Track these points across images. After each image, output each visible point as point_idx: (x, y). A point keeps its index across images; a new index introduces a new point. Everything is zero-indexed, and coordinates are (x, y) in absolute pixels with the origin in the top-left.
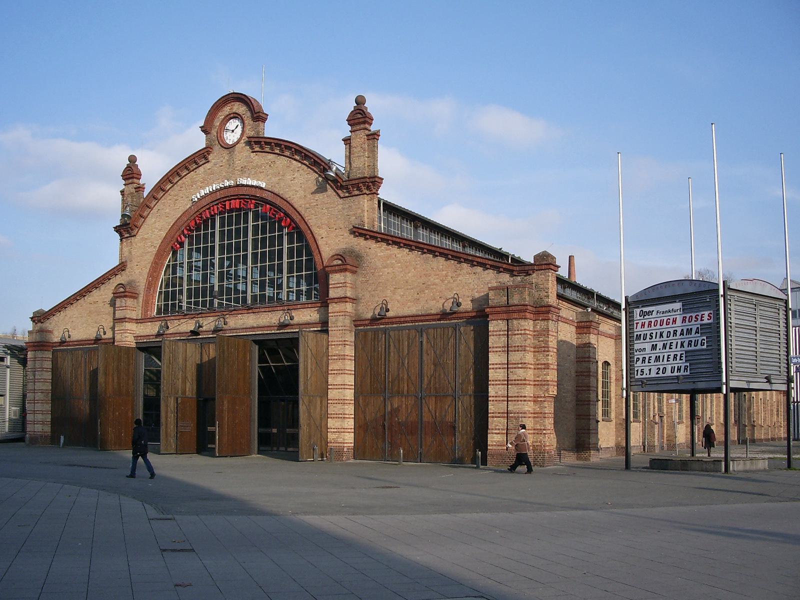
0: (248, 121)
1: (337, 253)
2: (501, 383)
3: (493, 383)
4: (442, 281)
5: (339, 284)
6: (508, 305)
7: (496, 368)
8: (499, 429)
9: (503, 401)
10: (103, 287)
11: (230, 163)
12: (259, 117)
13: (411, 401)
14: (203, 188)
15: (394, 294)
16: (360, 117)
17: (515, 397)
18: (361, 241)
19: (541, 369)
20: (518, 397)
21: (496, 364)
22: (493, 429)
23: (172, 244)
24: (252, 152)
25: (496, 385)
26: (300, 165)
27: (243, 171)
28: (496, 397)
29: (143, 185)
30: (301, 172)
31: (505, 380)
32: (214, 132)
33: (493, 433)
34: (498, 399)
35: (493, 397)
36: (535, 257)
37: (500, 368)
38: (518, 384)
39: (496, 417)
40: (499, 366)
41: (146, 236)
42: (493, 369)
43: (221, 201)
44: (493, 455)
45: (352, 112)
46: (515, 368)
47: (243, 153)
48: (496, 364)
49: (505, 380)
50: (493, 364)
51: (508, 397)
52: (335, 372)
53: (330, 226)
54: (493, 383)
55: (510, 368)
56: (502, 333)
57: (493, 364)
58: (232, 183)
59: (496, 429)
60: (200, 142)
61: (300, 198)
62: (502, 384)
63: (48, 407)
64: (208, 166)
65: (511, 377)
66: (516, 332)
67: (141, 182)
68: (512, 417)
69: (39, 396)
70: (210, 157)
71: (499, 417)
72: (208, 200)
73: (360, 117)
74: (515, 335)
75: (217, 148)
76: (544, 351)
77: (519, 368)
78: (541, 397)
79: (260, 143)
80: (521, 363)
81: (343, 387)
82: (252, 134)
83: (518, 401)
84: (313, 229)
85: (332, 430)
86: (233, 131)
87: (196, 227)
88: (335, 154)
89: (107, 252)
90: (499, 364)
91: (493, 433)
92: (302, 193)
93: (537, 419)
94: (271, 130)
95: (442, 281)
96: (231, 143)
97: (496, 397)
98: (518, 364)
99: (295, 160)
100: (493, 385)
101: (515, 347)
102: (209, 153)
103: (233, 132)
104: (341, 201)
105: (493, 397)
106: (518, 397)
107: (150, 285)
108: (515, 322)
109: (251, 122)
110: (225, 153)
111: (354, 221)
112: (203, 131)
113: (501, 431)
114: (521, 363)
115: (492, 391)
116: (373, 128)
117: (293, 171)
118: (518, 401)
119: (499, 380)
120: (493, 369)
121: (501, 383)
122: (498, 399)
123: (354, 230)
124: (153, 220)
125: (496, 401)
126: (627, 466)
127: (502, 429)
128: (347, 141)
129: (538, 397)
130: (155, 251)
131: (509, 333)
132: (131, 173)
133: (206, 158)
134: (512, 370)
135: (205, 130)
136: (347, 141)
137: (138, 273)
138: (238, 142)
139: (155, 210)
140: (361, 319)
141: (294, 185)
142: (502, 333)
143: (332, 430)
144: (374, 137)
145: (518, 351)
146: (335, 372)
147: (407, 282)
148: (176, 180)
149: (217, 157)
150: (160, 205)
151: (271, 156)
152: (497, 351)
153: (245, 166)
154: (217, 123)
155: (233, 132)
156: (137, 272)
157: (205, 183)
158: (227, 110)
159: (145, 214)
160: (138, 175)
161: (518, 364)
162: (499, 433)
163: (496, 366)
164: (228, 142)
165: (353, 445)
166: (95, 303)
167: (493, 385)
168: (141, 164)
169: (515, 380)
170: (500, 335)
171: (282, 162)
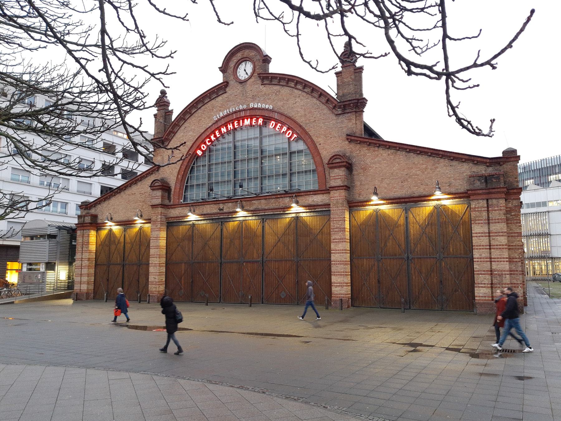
1: (334, 154)
2: (484, 247)
3: (476, 247)
4: (423, 172)
7: (479, 236)
8: (485, 284)
9: (486, 261)
10: (139, 184)
12: (267, 60)
15: (382, 182)
16: (348, 56)
17: (498, 258)
18: (352, 146)
19: (515, 236)
20: (501, 258)
21: (479, 233)
22: (479, 284)
24: (262, 85)
25: (480, 249)
26: (300, 92)
27: (254, 98)
28: (480, 258)
29: (172, 110)
30: (301, 97)
31: (487, 246)
32: (230, 71)
33: (479, 287)
34: (482, 260)
35: (478, 258)
36: (504, 153)
37: (482, 236)
38: (500, 248)
39: (481, 274)
40: (483, 235)
42: (476, 237)
45: (343, 53)
46: (497, 236)
48: (479, 233)
49: (487, 246)
50: (476, 233)
51: (491, 258)
52: (337, 241)
54: (476, 247)
55: (492, 236)
56: (483, 209)
57: (476, 233)
58: (245, 107)
59: (482, 284)
60: (219, 78)
61: (301, 116)
62: (486, 249)
63: (92, 271)
64: (225, 95)
65: (493, 243)
66: (496, 208)
67: (170, 108)
68: (496, 274)
69: (86, 263)
70: (227, 90)
71: (484, 274)
74: (495, 210)
75: (232, 83)
76: (517, 223)
77: (500, 236)
78: (516, 258)
80: (502, 232)
81: (344, 251)
82: (261, 71)
83: (501, 261)
84: (314, 138)
85: (336, 284)
86: (245, 70)
88: (329, 84)
90: (482, 233)
91: (479, 287)
92: (303, 113)
93: (513, 276)
94: (273, 68)
95: (423, 172)
96: (243, 79)
97: (480, 258)
98: (499, 232)
99: (297, 89)
100: (477, 249)
101: (495, 219)
103: (245, 70)
104: (334, 118)
105: (478, 258)
106: (501, 258)
108: (494, 201)
110: (239, 86)
112: (220, 71)
113: (486, 285)
114: (502, 232)
115: (476, 254)
117: (295, 97)
118: (501, 261)
119: (483, 246)
120: (476, 237)
121: (484, 247)
122: (482, 260)
123: (349, 137)
125: (481, 261)
127: (488, 284)
129: (513, 258)
131: (490, 209)
132: (162, 103)
134: (494, 238)
138: (250, 78)
139: (182, 128)
140: (356, 201)
141: (298, 105)
142: (483, 209)
143: (336, 284)
145: (498, 223)
146: (337, 241)
147: (392, 174)
148: (206, 101)
149: (233, 90)
150: (186, 124)
151: (277, 88)
152: (479, 223)
153: (256, 95)
155: (245, 70)
158: (239, 55)
159: (175, 130)
160: (167, 104)
161: (499, 232)
162: (484, 287)
163: (479, 235)
164: (240, 78)
165: (350, 295)
166: (132, 194)
167: (477, 249)
168: (170, 97)
169: (497, 245)
170: (481, 211)
171: (285, 91)
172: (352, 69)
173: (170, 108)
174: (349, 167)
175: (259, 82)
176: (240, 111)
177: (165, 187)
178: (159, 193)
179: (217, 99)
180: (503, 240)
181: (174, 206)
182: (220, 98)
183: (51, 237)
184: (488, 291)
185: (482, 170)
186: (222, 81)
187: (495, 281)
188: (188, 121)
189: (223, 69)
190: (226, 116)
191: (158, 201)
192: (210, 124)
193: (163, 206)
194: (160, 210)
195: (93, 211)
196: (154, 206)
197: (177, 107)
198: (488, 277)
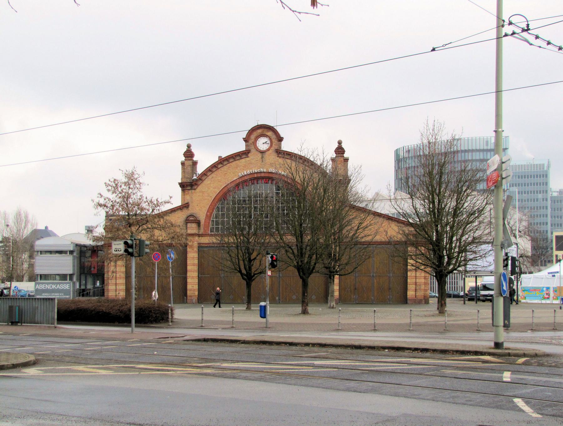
12: (280, 139)
16: (340, 150)
32: (251, 142)
41: (203, 190)
44: (410, 300)
47: (271, 157)
64: (247, 159)
67: (195, 159)
70: (249, 155)
72: (251, 177)
73: (340, 150)
75: (253, 151)
79: (280, 152)
94: (286, 146)
102: (249, 153)
103: (263, 144)
107: (208, 217)
109: (276, 142)
110: (260, 155)
124: (209, 182)
133: (247, 155)
135: (246, 140)
138: (268, 150)
139: (210, 177)
144: (346, 160)
149: (254, 157)
150: (213, 175)
154: (253, 137)
156: (197, 209)
158: (259, 131)
172: (342, 159)
173: (195, 159)
176: (261, 173)
179: (241, 160)
182: (243, 160)
183: (71, 252)
184: (413, 293)
186: (244, 149)
187: (417, 288)
188: (216, 173)
190: (251, 174)
192: (235, 179)
198: (414, 286)
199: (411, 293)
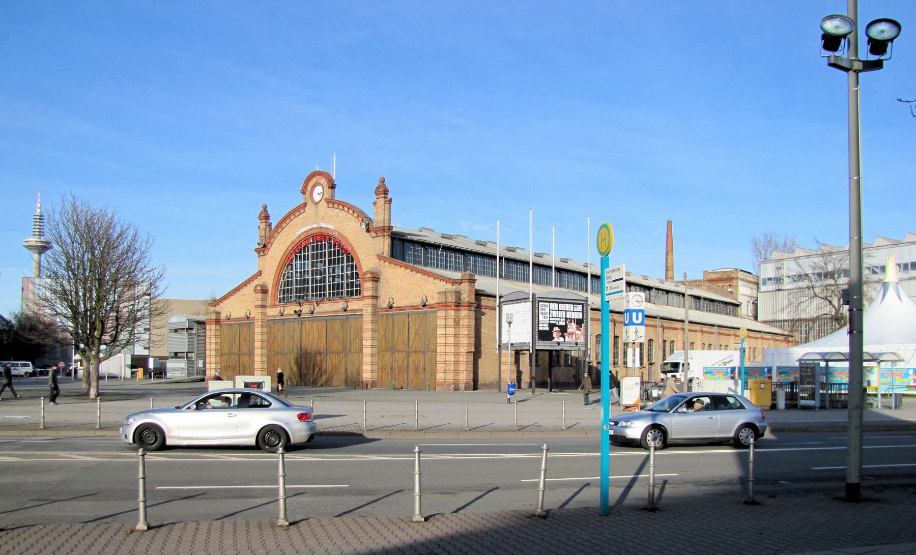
0: (326, 188)
5: (367, 288)
6: (446, 302)
11: (316, 212)
13: (404, 354)
14: (302, 227)
23: (287, 262)
43: (314, 237)
53: (369, 251)
75: (310, 204)
87: (299, 250)
89: (252, 265)
107: (276, 285)
110: (314, 206)
111: (378, 252)
116: (389, 196)
126: (475, 385)
128: (375, 203)
130: (277, 264)
135: (303, 192)
136: (375, 203)
137: (268, 279)
149: (310, 209)
154: (309, 188)
157: (304, 225)
158: (314, 180)
171: (343, 214)
174: (376, 279)
175: (326, 204)
177: (264, 291)
178: (260, 295)
180: (451, 340)
181: (271, 306)
185: (449, 286)
189: (303, 192)
191: (260, 303)
193: (263, 307)
194: (260, 310)
195: (217, 309)
196: (256, 307)
197: (274, 221)
199: (440, 376)
